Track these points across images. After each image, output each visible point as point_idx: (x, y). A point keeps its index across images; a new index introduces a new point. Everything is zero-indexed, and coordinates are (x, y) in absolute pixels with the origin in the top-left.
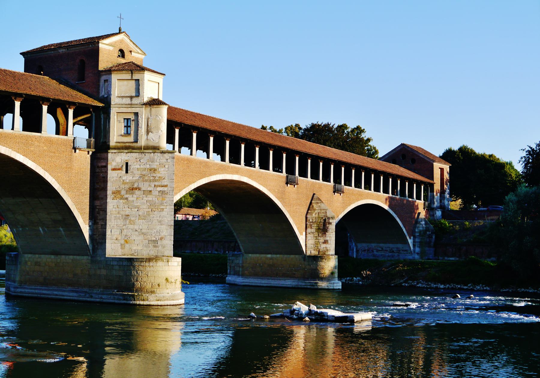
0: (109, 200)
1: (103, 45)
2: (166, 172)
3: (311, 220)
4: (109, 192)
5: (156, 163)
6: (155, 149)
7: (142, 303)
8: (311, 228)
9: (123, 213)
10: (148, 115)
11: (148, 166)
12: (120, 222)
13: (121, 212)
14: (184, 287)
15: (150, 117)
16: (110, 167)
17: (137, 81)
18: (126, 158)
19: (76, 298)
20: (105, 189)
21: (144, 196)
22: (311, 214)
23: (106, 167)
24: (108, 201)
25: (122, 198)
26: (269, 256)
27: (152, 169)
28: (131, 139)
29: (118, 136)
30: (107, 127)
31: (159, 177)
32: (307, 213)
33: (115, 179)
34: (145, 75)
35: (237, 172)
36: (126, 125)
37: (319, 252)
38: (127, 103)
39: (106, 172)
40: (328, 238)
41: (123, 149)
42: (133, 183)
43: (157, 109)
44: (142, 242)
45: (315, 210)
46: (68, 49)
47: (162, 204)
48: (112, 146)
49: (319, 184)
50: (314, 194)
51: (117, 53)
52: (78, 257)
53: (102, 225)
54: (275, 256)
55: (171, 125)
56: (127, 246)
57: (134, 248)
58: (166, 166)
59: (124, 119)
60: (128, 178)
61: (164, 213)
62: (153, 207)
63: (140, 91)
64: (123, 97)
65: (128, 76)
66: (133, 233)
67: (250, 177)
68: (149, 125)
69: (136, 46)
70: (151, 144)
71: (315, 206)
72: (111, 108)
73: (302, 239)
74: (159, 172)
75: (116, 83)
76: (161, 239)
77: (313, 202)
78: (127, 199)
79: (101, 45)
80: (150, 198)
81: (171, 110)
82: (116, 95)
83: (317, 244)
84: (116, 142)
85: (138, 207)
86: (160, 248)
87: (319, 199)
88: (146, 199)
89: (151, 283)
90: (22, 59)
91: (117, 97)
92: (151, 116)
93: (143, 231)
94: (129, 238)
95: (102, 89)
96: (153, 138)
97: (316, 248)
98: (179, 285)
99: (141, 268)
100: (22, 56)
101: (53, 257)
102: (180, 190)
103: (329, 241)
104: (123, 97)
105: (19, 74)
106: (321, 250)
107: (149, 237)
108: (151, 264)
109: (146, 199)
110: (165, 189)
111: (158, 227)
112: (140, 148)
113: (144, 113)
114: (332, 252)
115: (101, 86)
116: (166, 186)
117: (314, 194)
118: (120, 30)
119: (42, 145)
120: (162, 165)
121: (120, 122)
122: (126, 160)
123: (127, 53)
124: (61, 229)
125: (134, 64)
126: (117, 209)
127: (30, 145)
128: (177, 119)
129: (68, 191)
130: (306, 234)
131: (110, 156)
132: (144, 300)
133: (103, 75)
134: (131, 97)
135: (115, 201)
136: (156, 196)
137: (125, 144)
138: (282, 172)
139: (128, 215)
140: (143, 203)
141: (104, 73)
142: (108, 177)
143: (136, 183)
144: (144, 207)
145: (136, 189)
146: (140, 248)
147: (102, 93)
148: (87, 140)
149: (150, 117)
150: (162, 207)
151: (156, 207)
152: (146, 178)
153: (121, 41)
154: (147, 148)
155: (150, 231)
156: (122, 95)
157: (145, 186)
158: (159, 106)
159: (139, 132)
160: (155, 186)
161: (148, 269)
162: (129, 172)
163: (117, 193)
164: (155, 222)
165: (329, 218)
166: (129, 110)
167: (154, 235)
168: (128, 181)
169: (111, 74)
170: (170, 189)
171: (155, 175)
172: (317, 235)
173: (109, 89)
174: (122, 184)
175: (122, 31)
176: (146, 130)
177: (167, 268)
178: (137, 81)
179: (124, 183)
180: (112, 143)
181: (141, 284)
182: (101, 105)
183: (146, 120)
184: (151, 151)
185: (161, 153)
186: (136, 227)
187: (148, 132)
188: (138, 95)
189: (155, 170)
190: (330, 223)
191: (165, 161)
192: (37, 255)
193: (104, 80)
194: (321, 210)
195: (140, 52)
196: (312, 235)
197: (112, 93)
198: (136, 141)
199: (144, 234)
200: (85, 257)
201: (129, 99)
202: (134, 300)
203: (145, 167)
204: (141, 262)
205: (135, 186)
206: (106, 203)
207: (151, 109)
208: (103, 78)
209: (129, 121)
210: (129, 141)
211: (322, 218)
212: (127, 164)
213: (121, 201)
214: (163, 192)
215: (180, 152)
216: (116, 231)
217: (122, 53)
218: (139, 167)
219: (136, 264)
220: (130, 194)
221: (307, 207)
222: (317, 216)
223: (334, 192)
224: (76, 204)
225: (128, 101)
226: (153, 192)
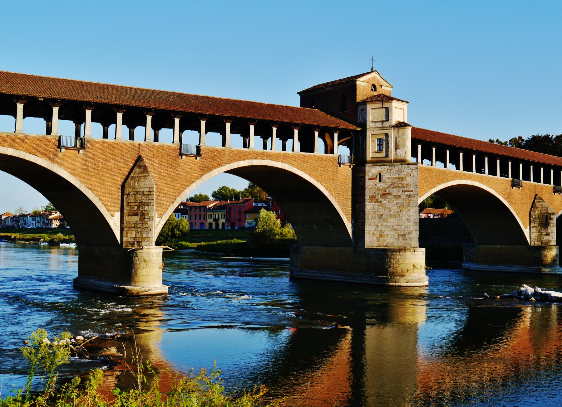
0: (367, 203)
1: (360, 82)
2: (411, 180)
3: (534, 216)
4: (367, 197)
5: (403, 173)
6: (403, 162)
7: (394, 284)
8: (535, 223)
9: (378, 213)
11: (397, 176)
12: (376, 220)
13: (377, 213)
14: (427, 273)
15: (397, 136)
16: (367, 177)
17: (388, 108)
18: (380, 170)
19: (342, 280)
20: (364, 195)
21: (394, 199)
22: (534, 211)
23: (364, 177)
24: (366, 204)
25: (377, 202)
26: (499, 246)
27: (401, 177)
28: (383, 154)
29: (373, 153)
30: (364, 146)
31: (406, 184)
32: (531, 210)
33: (371, 186)
34: (393, 103)
35: (470, 178)
36: (379, 144)
37: (542, 243)
38: (379, 126)
39: (364, 182)
40: (550, 231)
41: (377, 163)
42: (385, 190)
43: (403, 130)
44: (393, 236)
45: (537, 208)
46: (332, 87)
47: (409, 205)
49: (541, 186)
50: (536, 195)
51: (370, 88)
52: (344, 248)
53: (362, 223)
54: (503, 246)
55: (415, 143)
56: (382, 239)
57: (388, 241)
58: (412, 175)
59: (377, 139)
60: (382, 185)
61: (411, 213)
62: (401, 207)
64: (376, 122)
65: (380, 105)
66: (386, 229)
67: (481, 182)
68: (397, 143)
69: (386, 81)
70: (399, 158)
71: (537, 204)
72: (367, 131)
73: (526, 232)
74: (406, 180)
75: (370, 111)
76: (409, 233)
77: (536, 201)
78: (381, 202)
79: (357, 82)
80: (399, 201)
81: (414, 130)
83: (540, 236)
84: (371, 158)
85: (390, 208)
86: (408, 240)
87: (541, 199)
88: (396, 202)
89: (401, 269)
90: (299, 97)
91: (371, 122)
92: (398, 136)
93: (394, 227)
94: (383, 233)
95: (360, 116)
97: (539, 240)
98: (424, 270)
99: (393, 257)
100: (298, 95)
101: (324, 248)
102: (423, 194)
103: (551, 234)
104: (376, 122)
105: (296, 108)
106: (544, 241)
107: (399, 231)
108: (401, 253)
109: (396, 202)
110: (411, 193)
111: (406, 224)
112: (390, 162)
113: (393, 134)
114: (554, 243)
115: (359, 114)
116: (412, 191)
117: (536, 195)
118: (372, 69)
119: (315, 162)
120: (408, 174)
121: (374, 142)
122: (380, 172)
123: (378, 87)
124: (331, 227)
125: (384, 95)
126: (373, 210)
127: (306, 162)
128: (419, 137)
129: (335, 197)
130: (530, 228)
131: (367, 168)
132: (396, 282)
133: (360, 105)
134: (383, 122)
135: (372, 204)
136: (404, 199)
137: (378, 159)
138: (508, 177)
139: (382, 215)
140: (394, 205)
141: (360, 104)
142: (366, 185)
143: (388, 189)
144: (395, 208)
145: (388, 194)
146: (392, 240)
147: (360, 120)
148: (349, 157)
149: (397, 136)
150: (409, 208)
151: (404, 208)
152: (396, 185)
153: (374, 78)
154: (396, 161)
155: (399, 227)
156: (375, 121)
157: (395, 192)
158: (405, 128)
159: (389, 149)
160: (403, 191)
161: (399, 257)
163: (373, 197)
164: (404, 220)
165: (550, 215)
166: (381, 132)
167: (403, 230)
168: (381, 188)
169: (366, 104)
170: (415, 193)
171: (403, 183)
172: (540, 229)
174: (377, 190)
175: (374, 70)
176: (394, 147)
177: (414, 256)
178: (387, 109)
179: (378, 189)
180: (368, 158)
181: (393, 269)
182: (359, 129)
183: (395, 139)
184: (399, 164)
185: (407, 165)
186: (389, 224)
187: (396, 148)
188: (387, 119)
189: (403, 178)
190: (552, 219)
191: (411, 171)
192: (313, 247)
193: (361, 110)
194: (543, 207)
195: (388, 85)
196: (535, 229)
197: (367, 119)
198: (387, 156)
199: (395, 229)
200: (349, 248)
201: (380, 123)
202: (388, 282)
203: (394, 176)
204: (393, 252)
205: (387, 191)
206: (364, 206)
207: (398, 130)
208: (361, 108)
210: (381, 156)
211: (544, 214)
212: (380, 174)
213: (377, 204)
214: (409, 196)
215: (422, 163)
216: (373, 228)
217: (374, 88)
218: (390, 176)
219: (389, 253)
220: (383, 198)
221: (531, 206)
222: (539, 212)
223: (554, 192)
224: (342, 207)
225: (380, 125)
226: (401, 196)
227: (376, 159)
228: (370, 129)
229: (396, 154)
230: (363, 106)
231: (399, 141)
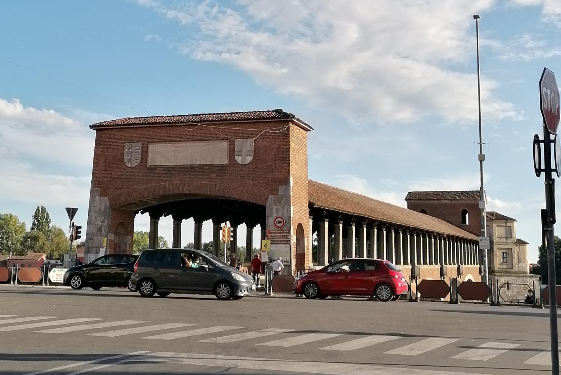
10: (518, 250)
15: (519, 251)
18: (508, 280)
38: (504, 242)
43: (523, 246)
46: (451, 201)
48: (496, 271)
63: (512, 234)
64: (501, 238)
70: (521, 270)
72: (494, 245)
82: (496, 236)
84: (499, 268)
96: (522, 266)
104: (501, 238)
112: (515, 273)
113: (516, 249)
149: (519, 251)
152: (522, 294)
154: (520, 272)
156: (500, 236)
162: (510, 289)
173: (491, 232)
176: (517, 260)
187: (519, 261)
188: (511, 236)
197: (494, 234)
201: (505, 239)
209: (505, 254)
227: (502, 270)
228: (497, 243)
229: (518, 266)
230: (490, 223)
231: (521, 257)
